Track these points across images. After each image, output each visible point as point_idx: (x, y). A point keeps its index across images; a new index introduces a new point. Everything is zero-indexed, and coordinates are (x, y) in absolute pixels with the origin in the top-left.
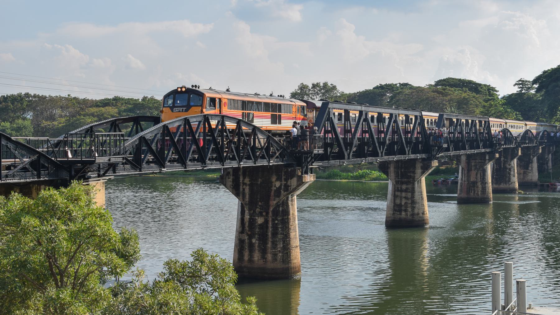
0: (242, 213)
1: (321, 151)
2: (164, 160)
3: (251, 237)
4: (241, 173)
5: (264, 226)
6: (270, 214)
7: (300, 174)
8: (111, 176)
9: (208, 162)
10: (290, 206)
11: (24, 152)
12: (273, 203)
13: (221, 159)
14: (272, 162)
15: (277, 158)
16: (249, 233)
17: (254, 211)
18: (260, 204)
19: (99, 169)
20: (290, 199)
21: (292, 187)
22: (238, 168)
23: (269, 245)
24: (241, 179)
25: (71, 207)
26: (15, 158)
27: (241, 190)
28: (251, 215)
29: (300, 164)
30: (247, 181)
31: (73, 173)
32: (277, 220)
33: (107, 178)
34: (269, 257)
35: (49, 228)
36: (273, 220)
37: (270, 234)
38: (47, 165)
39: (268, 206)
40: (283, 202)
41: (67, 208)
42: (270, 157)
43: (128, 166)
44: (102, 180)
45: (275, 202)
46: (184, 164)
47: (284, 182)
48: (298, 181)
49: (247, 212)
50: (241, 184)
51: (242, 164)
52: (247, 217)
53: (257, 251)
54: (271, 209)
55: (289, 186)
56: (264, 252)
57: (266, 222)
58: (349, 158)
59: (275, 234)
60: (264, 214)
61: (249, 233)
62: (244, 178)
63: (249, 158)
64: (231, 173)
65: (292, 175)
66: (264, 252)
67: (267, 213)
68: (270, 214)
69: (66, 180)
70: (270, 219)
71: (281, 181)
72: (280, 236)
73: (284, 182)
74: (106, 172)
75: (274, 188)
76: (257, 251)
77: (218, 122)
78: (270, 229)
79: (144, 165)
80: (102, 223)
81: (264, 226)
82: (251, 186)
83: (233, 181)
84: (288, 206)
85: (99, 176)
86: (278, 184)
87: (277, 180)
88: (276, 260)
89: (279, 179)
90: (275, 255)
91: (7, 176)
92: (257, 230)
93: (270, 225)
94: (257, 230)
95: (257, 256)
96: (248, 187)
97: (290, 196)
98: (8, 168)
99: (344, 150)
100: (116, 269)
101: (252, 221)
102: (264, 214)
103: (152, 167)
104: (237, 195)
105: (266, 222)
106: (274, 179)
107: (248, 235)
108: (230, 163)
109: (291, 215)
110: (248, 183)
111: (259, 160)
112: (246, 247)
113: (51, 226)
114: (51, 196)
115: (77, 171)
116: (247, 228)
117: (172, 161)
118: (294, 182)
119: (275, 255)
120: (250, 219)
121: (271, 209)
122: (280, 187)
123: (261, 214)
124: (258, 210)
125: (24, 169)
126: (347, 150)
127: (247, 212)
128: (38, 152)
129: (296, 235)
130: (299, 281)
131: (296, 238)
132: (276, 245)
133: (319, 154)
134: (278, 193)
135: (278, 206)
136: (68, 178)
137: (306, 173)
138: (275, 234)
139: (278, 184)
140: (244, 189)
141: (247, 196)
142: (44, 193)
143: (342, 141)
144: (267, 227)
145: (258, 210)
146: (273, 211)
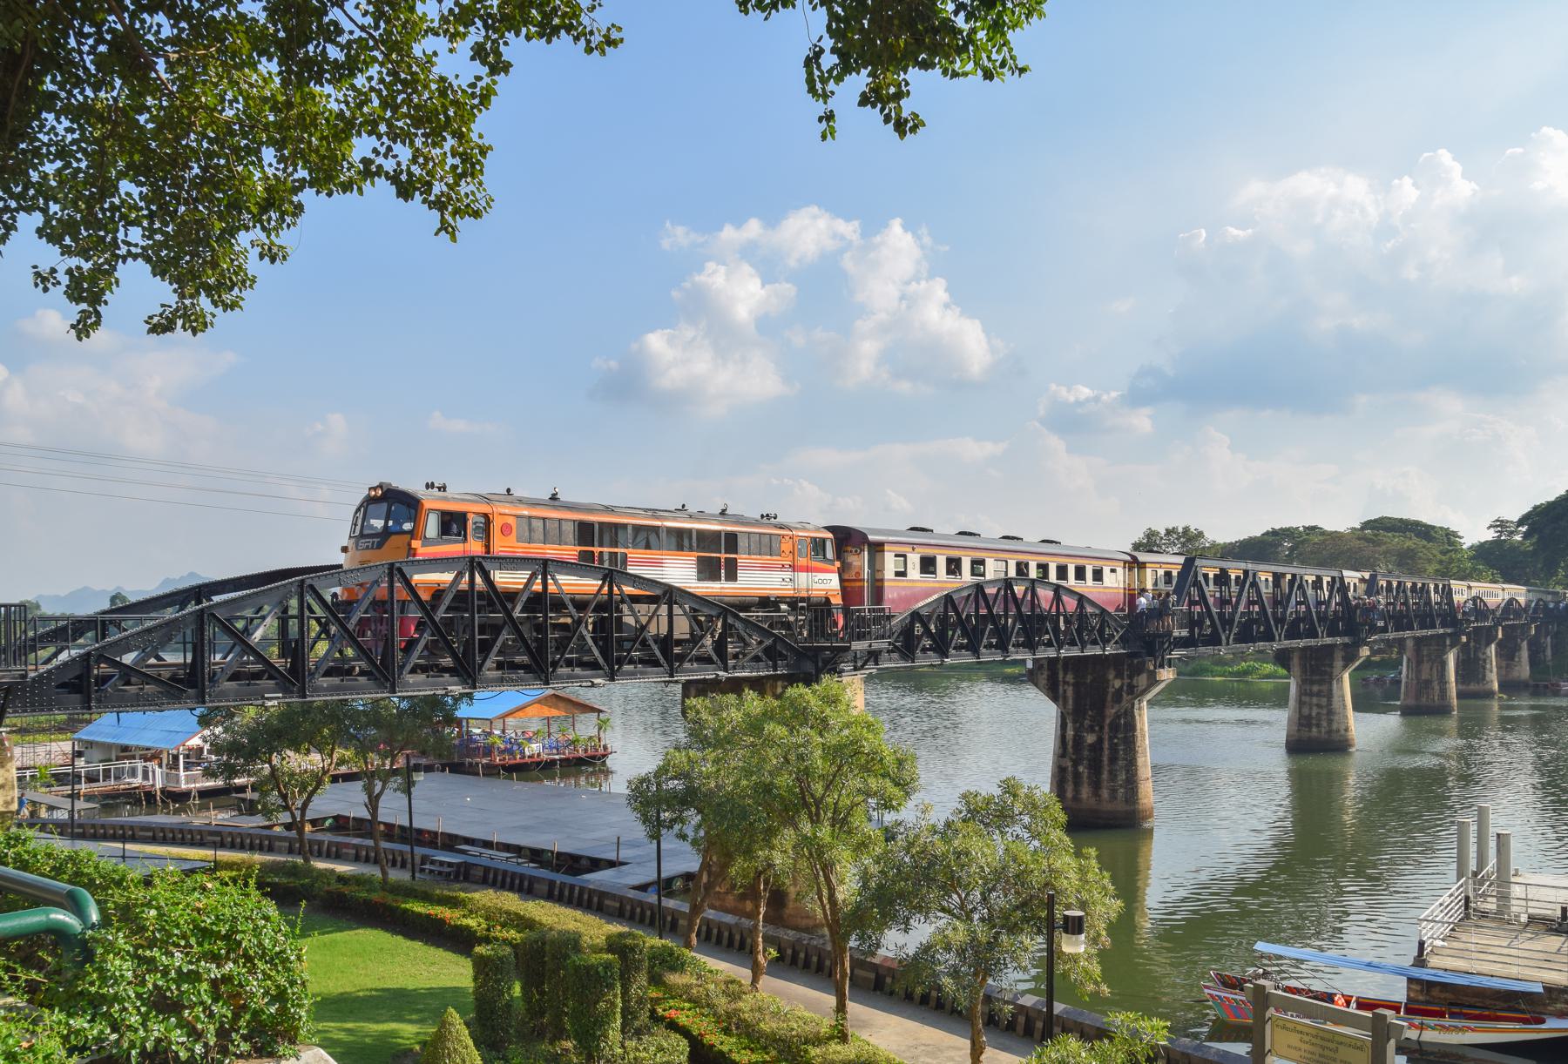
0: (1063, 726)
1: (1185, 633)
2: (948, 645)
3: (1076, 763)
4: (1060, 666)
5: (1097, 747)
6: (1106, 729)
7: (1152, 668)
8: (871, 669)
9: (1011, 648)
12: (1111, 712)
13: (1030, 645)
14: (1109, 650)
15: (1116, 643)
17: (1082, 725)
19: (855, 659)
20: (1136, 706)
21: (1140, 688)
22: (1057, 659)
23: (1105, 776)
24: (1061, 676)
25: (828, 711)
28: (1076, 730)
29: (1151, 653)
30: (1070, 678)
31: (820, 664)
34: (1105, 793)
35: (800, 740)
36: (1111, 739)
37: (1105, 759)
39: (1103, 718)
40: (1126, 713)
42: (1106, 641)
43: (895, 655)
44: (861, 675)
46: (976, 653)
47: (1127, 681)
49: (1070, 725)
52: (1070, 733)
53: (1086, 785)
54: (1108, 721)
56: (1096, 786)
57: (1100, 740)
58: (1228, 644)
59: (1113, 759)
62: (1065, 674)
65: (1139, 670)
66: (1096, 786)
67: (1102, 728)
68: (1106, 729)
69: (810, 674)
71: (1122, 679)
73: (1127, 681)
74: (865, 664)
75: (1111, 690)
77: (1027, 589)
78: (1106, 752)
79: (918, 653)
80: (870, 736)
81: (1097, 747)
82: (1076, 685)
84: (1133, 717)
85: (856, 669)
86: (1117, 683)
87: (1116, 677)
88: (1116, 798)
89: (1119, 675)
90: (1113, 791)
91: (734, 668)
92: (1086, 753)
93: (1106, 745)
94: (1086, 753)
95: (1085, 792)
97: (1136, 702)
98: (735, 656)
99: (1220, 631)
100: (891, 800)
101: (1078, 740)
103: (930, 657)
104: (1055, 699)
105: (1100, 740)
106: (1111, 676)
107: (1071, 759)
110: (1072, 681)
112: (1070, 777)
115: (826, 662)
116: (1070, 749)
117: (959, 648)
118: (1142, 680)
119: (1113, 791)
120: (1075, 736)
121: (1108, 721)
122: (1122, 687)
123: (1091, 729)
124: (1087, 722)
125: (757, 659)
127: (1070, 725)
130: (1151, 831)
131: (1146, 766)
132: (1116, 776)
133: (1181, 638)
135: (1118, 717)
137: (1162, 666)
139: (1117, 683)
140: (1065, 691)
141: (1070, 702)
142: (792, 692)
143: (1216, 617)
144: (1101, 749)
145: (1087, 722)
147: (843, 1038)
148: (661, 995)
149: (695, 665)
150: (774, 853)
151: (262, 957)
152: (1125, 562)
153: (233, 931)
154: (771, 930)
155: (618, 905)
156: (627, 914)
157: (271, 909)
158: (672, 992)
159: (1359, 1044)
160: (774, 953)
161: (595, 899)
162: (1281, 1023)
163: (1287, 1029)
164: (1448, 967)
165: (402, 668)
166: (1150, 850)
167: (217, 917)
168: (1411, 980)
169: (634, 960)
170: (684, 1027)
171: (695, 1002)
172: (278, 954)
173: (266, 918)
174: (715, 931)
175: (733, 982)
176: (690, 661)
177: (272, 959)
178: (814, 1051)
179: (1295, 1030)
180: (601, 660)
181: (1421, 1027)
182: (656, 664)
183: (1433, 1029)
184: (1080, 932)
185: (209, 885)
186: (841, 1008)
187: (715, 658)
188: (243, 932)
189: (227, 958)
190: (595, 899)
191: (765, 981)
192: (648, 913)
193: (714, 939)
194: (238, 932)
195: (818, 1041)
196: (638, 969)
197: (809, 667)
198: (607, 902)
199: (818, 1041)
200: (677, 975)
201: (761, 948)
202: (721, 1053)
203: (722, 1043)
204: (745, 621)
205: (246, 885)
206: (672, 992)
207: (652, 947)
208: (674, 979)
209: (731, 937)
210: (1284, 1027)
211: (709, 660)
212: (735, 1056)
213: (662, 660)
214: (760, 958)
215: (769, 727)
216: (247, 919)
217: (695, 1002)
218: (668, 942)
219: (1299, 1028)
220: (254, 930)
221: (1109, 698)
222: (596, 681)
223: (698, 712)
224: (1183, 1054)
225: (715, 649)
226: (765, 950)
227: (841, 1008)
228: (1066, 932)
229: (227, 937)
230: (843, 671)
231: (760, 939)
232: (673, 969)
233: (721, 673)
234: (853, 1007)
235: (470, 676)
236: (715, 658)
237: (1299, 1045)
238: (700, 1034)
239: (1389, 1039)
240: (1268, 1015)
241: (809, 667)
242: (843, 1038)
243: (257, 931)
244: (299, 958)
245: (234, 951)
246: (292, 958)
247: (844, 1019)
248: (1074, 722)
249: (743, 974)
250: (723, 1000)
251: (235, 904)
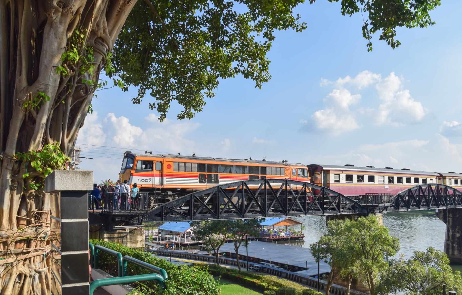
0: (448, 231)
2: (410, 205)
3: (453, 243)
4: (447, 212)
9: (431, 206)
13: (437, 205)
16: (452, 241)
17: (455, 231)
19: (380, 209)
24: (447, 215)
25: (371, 225)
27: (447, 220)
28: (453, 232)
30: (451, 215)
33: (384, 213)
35: (363, 234)
41: (370, 225)
43: (392, 208)
46: (419, 207)
49: (451, 231)
50: (448, 217)
51: (448, 207)
52: (451, 233)
53: (456, 250)
61: (452, 241)
62: (449, 214)
63: (452, 204)
64: (442, 212)
69: (366, 214)
74: (383, 211)
76: (456, 250)
77: (436, 187)
79: (400, 207)
80: (385, 233)
82: (453, 218)
85: (380, 212)
91: (342, 212)
92: (456, 240)
96: (451, 219)
98: (343, 208)
101: (453, 236)
103: (404, 209)
104: (445, 222)
107: (451, 242)
110: (451, 216)
111: (457, 205)
112: (451, 247)
115: (371, 210)
116: (451, 239)
117: (413, 206)
120: (452, 234)
124: (457, 230)
125: (349, 209)
127: (451, 231)
128: (354, 202)
136: (367, 213)
140: (449, 220)
141: (451, 223)
142: (360, 219)
145: (457, 230)
149: (330, 211)
151: (209, 291)
152: (437, 176)
153: (202, 283)
157: (212, 277)
165: (245, 211)
167: (198, 279)
172: (213, 290)
173: (210, 280)
176: (329, 209)
177: (212, 291)
180: (302, 209)
182: (319, 210)
185: (196, 270)
187: (336, 208)
188: (204, 283)
189: (200, 290)
194: (203, 283)
197: (365, 211)
205: (205, 271)
211: (335, 209)
213: (320, 209)
216: (206, 280)
220: (207, 283)
222: (301, 215)
223: (331, 225)
225: (336, 206)
229: (200, 285)
230: (376, 213)
233: (338, 213)
235: (264, 213)
236: (336, 208)
241: (365, 211)
243: (208, 283)
244: (219, 291)
245: (202, 288)
246: (217, 291)
248: (452, 230)
251: (202, 276)
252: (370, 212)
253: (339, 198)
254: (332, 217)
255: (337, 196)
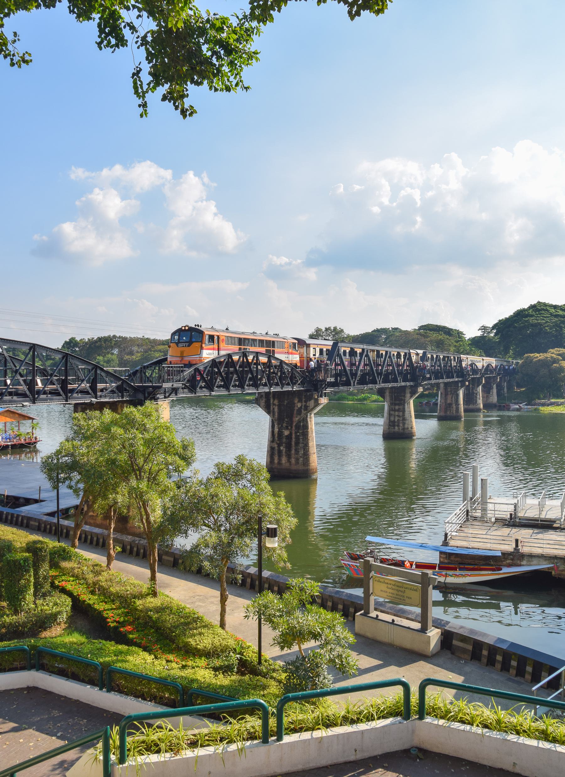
0: (273, 426)
1: (333, 380)
2: (213, 385)
3: (279, 446)
4: (271, 396)
6: (294, 428)
7: (316, 397)
8: (173, 397)
10: (309, 422)
11: (112, 379)
12: (296, 419)
13: (256, 386)
14: (295, 388)
15: (299, 384)
16: (278, 442)
17: (282, 426)
18: (286, 420)
19: (165, 392)
20: (309, 416)
21: (311, 407)
22: (269, 393)
23: (293, 452)
24: (272, 401)
25: (146, 421)
26: (106, 383)
27: (272, 409)
28: (279, 428)
29: (316, 390)
30: (276, 402)
31: (146, 395)
32: (299, 432)
33: (171, 399)
34: (293, 461)
35: (130, 436)
36: (296, 433)
37: (293, 443)
38: (128, 389)
40: (303, 419)
41: (143, 421)
42: (294, 384)
43: (186, 390)
44: (168, 401)
45: (297, 419)
46: (228, 389)
47: (304, 404)
48: (315, 402)
49: (276, 426)
51: (273, 389)
52: (276, 430)
53: (284, 456)
54: (294, 424)
55: (308, 407)
56: (289, 456)
57: (291, 434)
58: (354, 385)
59: (297, 443)
60: (289, 428)
61: (278, 442)
62: (274, 400)
63: (277, 384)
64: (264, 396)
65: (310, 398)
66: (289, 456)
67: (292, 427)
68: (294, 428)
69: (141, 400)
70: (294, 432)
71: (302, 403)
72: (301, 445)
73: (304, 404)
74: (170, 395)
75: (296, 408)
76: (284, 456)
77: (254, 357)
79: (198, 389)
80: (168, 434)
81: (289, 437)
82: (279, 406)
83: (266, 402)
84: (307, 422)
85: (165, 397)
86: (299, 405)
87: (299, 402)
89: (300, 401)
90: (297, 459)
91: (101, 397)
92: (284, 440)
93: (294, 436)
94: (284, 440)
95: (284, 460)
96: (277, 407)
97: (309, 414)
98: (102, 390)
99: (350, 378)
100: (178, 468)
101: (280, 434)
102: (289, 428)
103: (204, 391)
104: (269, 413)
105: (291, 434)
106: (296, 402)
107: (277, 444)
108: (263, 388)
109: (310, 429)
110: (277, 404)
111: (285, 386)
112: (276, 452)
113: (132, 434)
114: (131, 412)
115: (149, 394)
116: (276, 439)
118: (311, 403)
119: (297, 459)
120: (279, 431)
121: (294, 424)
122: (301, 407)
123: (287, 428)
124: (285, 425)
125: (113, 392)
126: (352, 379)
127: (276, 426)
129: (313, 444)
130: (316, 480)
131: (313, 447)
132: (298, 452)
133: (331, 382)
134: (299, 410)
135: (299, 422)
136: (143, 399)
137: (321, 396)
138: (297, 443)
139: (299, 405)
140: (274, 409)
141: (276, 414)
142: (128, 410)
143: (349, 372)
144: (291, 438)
145: (285, 425)
146: (296, 426)
147: (155, 594)
148: (57, 574)
149: (80, 395)
150: (118, 496)
154: (119, 536)
155: (37, 524)
156: (42, 529)
158: (64, 572)
159: (415, 588)
160: (119, 549)
161: (25, 521)
162: (377, 579)
163: (380, 582)
164: (459, 545)
166: (315, 489)
168: (441, 553)
169: (42, 555)
170: (69, 591)
171: (77, 577)
174: (89, 537)
175: (97, 565)
176: (77, 393)
178: (139, 602)
179: (384, 582)
181: (446, 576)
183: (451, 576)
184: (275, 536)
186: (153, 578)
187: (90, 391)
190: (25, 521)
191: (116, 564)
192: (54, 528)
193: (89, 541)
195: (141, 596)
196: (43, 561)
197: (141, 396)
198: (32, 523)
199: (141, 596)
200: (67, 563)
201: (112, 546)
202: (89, 605)
203: (89, 599)
204: (107, 373)
206: (64, 572)
207: (54, 547)
208: (65, 564)
209: (98, 540)
210: (379, 581)
211: (87, 393)
212: (96, 607)
213: (62, 393)
214: (112, 552)
215: (114, 429)
217: (77, 577)
218: (63, 544)
219: (386, 581)
221: (295, 412)
224: (330, 596)
226: (114, 548)
227: (153, 578)
228: (268, 536)
230: (158, 398)
231: (111, 542)
232: (65, 559)
233: (93, 399)
234: (158, 575)
236: (90, 391)
237: (386, 589)
238: (78, 595)
239: (429, 586)
240: (371, 575)
241: (141, 396)
242: (155, 594)
247: (155, 584)
248: (278, 424)
249: (102, 560)
250: (91, 575)
252: (148, 397)
253: (96, 372)
254: (84, 406)
255: (92, 370)
